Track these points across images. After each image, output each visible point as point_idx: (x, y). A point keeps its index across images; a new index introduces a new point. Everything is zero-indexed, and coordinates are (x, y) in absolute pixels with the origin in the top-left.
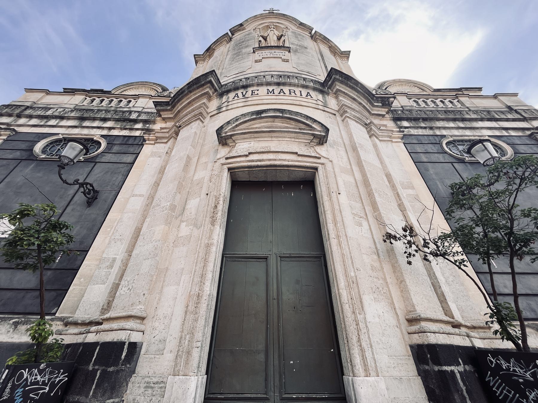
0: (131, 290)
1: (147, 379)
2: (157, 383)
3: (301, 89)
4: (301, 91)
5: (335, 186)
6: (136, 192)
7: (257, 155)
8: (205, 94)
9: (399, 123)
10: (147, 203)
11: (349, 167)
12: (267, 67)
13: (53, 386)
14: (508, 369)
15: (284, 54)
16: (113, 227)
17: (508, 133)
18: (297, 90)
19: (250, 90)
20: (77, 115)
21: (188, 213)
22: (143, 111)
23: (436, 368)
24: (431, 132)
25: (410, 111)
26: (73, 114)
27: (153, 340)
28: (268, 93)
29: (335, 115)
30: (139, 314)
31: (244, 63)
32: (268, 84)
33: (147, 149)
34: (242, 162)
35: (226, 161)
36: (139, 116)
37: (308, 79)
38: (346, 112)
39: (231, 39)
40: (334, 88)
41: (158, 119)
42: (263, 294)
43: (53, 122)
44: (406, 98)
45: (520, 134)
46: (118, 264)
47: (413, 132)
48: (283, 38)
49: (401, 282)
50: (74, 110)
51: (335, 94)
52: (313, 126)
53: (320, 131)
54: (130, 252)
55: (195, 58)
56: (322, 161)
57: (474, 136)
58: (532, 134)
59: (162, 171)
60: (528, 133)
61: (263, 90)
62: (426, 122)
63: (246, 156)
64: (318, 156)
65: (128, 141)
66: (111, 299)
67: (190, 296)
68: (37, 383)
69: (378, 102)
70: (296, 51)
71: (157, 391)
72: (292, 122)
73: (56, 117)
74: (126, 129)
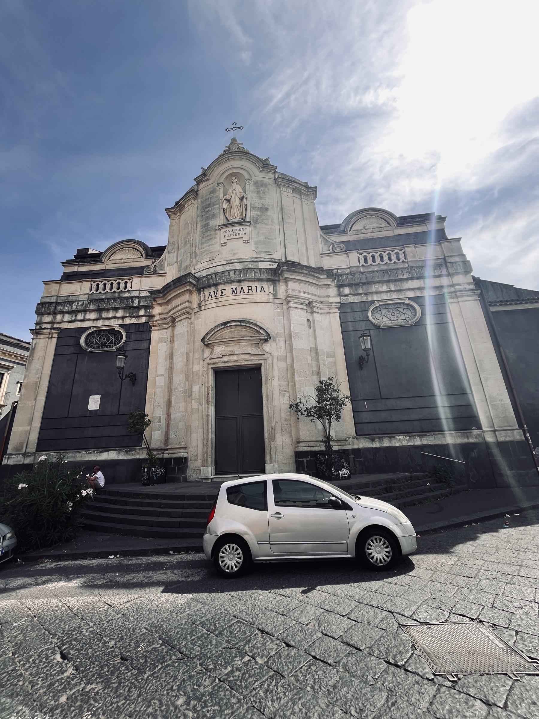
3: (256, 284)
4: (256, 287)
5: (271, 374)
6: (159, 373)
12: (232, 254)
13: (162, 473)
15: (244, 232)
18: (253, 285)
20: (95, 308)
22: (141, 295)
24: (362, 299)
25: (353, 274)
26: (91, 307)
28: (232, 294)
30: (184, 446)
32: (232, 282)
33: (155, 335)
36: (139, 302)
37: (263, 270)
38: (290, 301)
39: (197, 193)
41: (155, 303)
43: (80, 316)
46: (163, 422)
48: (245, 200)
49: (297, 426)
50: (90, 302)
54: (169, 415)
59: (171, 357)
61: (228, 289)
67: (203, 439)
68: (157, 472)
70: (256, 222)
71: (198, 472)
73: (81, 311)
74: (134, 317)
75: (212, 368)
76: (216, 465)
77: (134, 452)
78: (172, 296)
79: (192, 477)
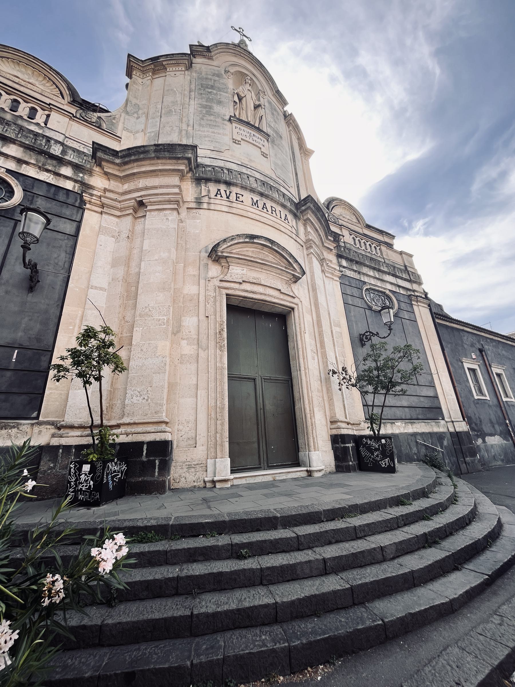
0: (147, 400)
1: (188, 463)
2: (198, 464)
7: (249, 284)
8: (179, 170)
9: (340, 260)
10: (120, 303)
11: (309, 307)
14: (370, 444)
16: (75, 324)
17: (399, 290)
19: (235, 190)
21: (187, 331)
23: (342, 445)
27: (181, 439)
29: (302, 246)
31: (220, 136)
34: (238, 290)
35: (220, 282)
40: (305, 215)
41: (97, 169)
42: (254, 406)
44: (348, 232)
45: (405, 293)
47: (349, 273)
51: (305, 221)
52: (294, 265)
53: (299, 273)
55: (129, 61)
56: (296, 301)
57: (382, 287)
58: (410, 295)
60: (409, 293)
61: (247, 197)
62: (357, 265)
63: (240, 283)
64: (294, 296)
65: (57, 195)
66: (108, 405)
69: (331, 236)
72: (277, 255)
74: (48, 171)
75: (227, 295)
76: (231, 455)
77: (15, 430)
78: (143, 169)
79: (183, 479)
